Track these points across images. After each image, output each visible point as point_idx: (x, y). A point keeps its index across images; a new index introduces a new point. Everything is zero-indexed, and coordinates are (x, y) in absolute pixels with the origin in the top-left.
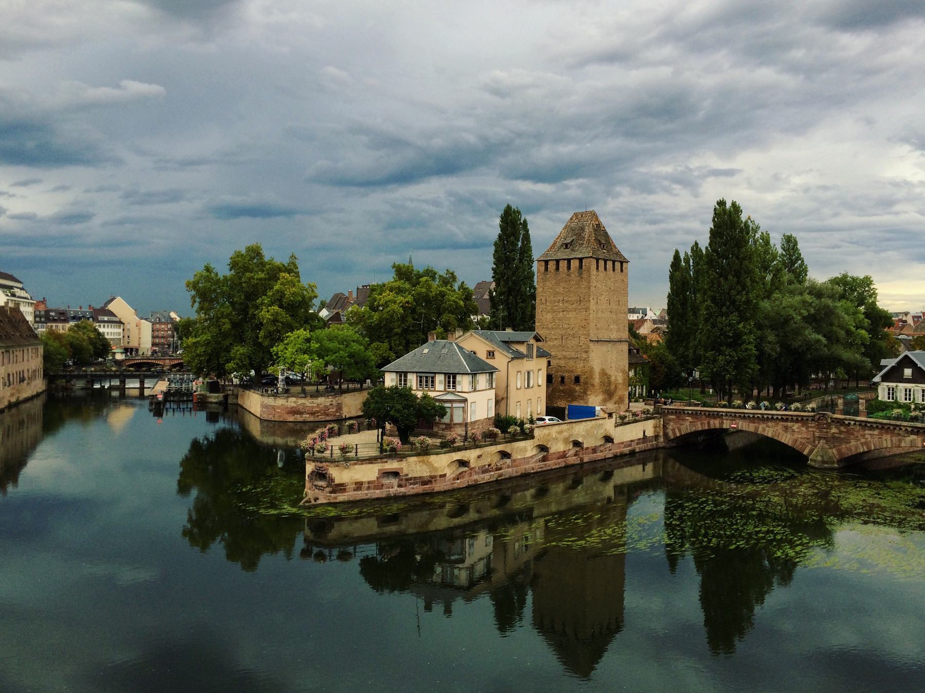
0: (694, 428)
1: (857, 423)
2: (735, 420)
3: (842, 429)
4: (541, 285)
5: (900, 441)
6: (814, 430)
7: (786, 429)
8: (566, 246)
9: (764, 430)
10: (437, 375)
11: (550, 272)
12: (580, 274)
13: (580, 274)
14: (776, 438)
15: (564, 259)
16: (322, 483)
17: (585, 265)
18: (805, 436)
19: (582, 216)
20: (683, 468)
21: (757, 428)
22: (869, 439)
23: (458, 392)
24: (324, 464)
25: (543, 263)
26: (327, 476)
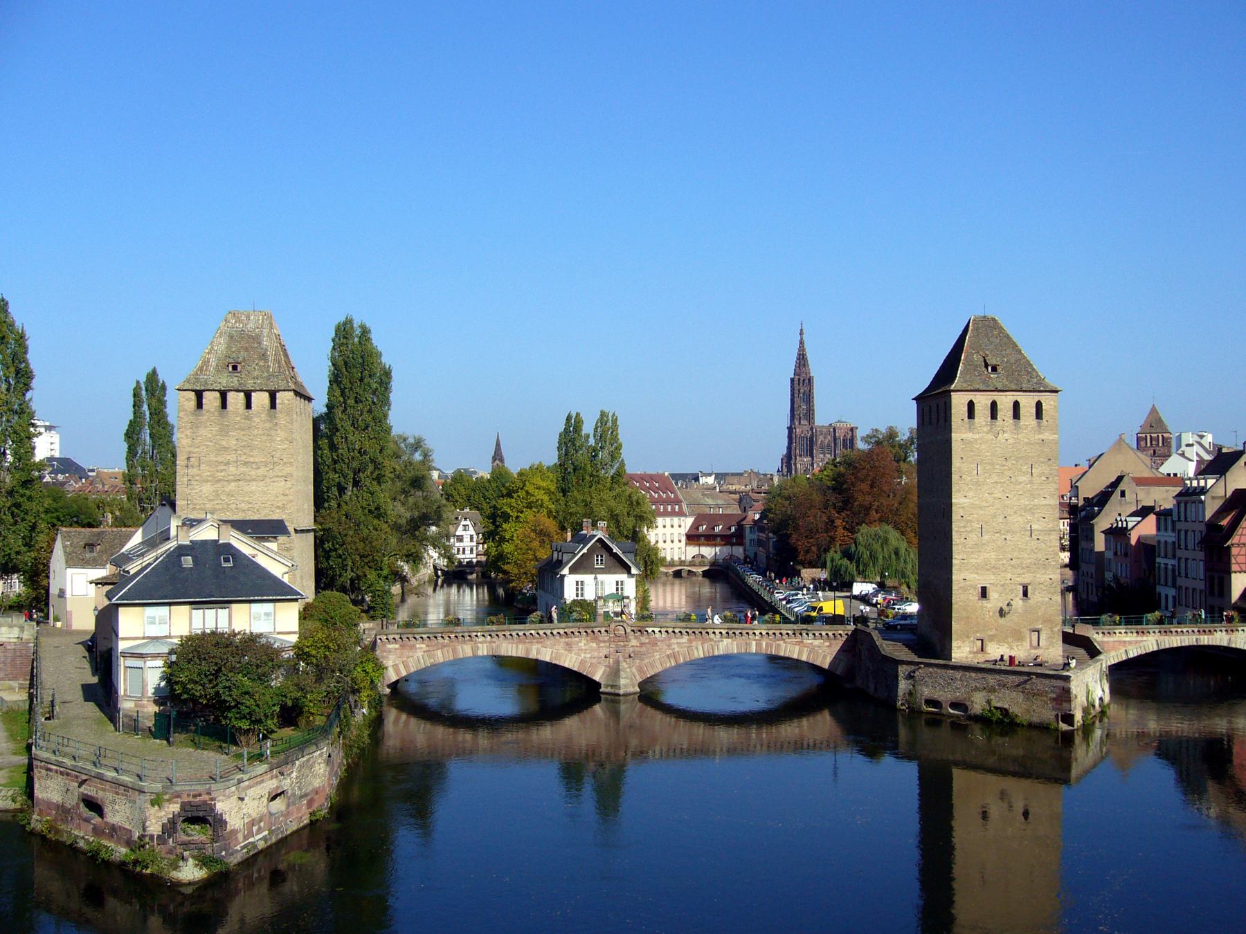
0: (432, 660)
1: (663, 630)
2: (494, 642)
3: (644, 639)
4: (188, 433)
6: (608, 644)
7: (569, 647)
11: (208, 411)
13: (272, 418)
17: (283, 403)
18: (596, 654)
20: (413, 721)
21: (528, 651)
22: (676, 650)
23: (279, 633)
25: (192, 395)
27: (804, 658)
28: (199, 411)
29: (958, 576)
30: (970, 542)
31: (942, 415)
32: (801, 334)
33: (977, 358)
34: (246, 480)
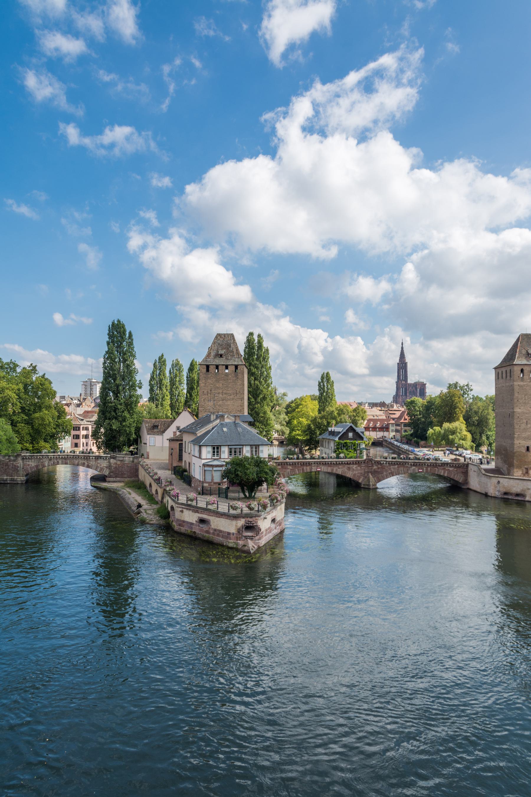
3: (379, 466)
4: (203, 381)
5: (408, 470)
7: (349, 469)
8: (221, 356)
9: (336, 470)
10: (244, 447)
12: (236, 376)
13: (236, 376)
14: (344, 475)
15: (223, 365)
16: (249, 534)
18: (360, 472)
19: (225, 336)
21: (332, 470)
24: (254, 519)
25: (205, 367)
26: (256, 527)
27: (446, 475)
28: (207, 373)
29: (516, 442)
30: (522, 428)
31: (508, 374)
32: (402, 344)
33: (524, 352)
34: (226, 400)
